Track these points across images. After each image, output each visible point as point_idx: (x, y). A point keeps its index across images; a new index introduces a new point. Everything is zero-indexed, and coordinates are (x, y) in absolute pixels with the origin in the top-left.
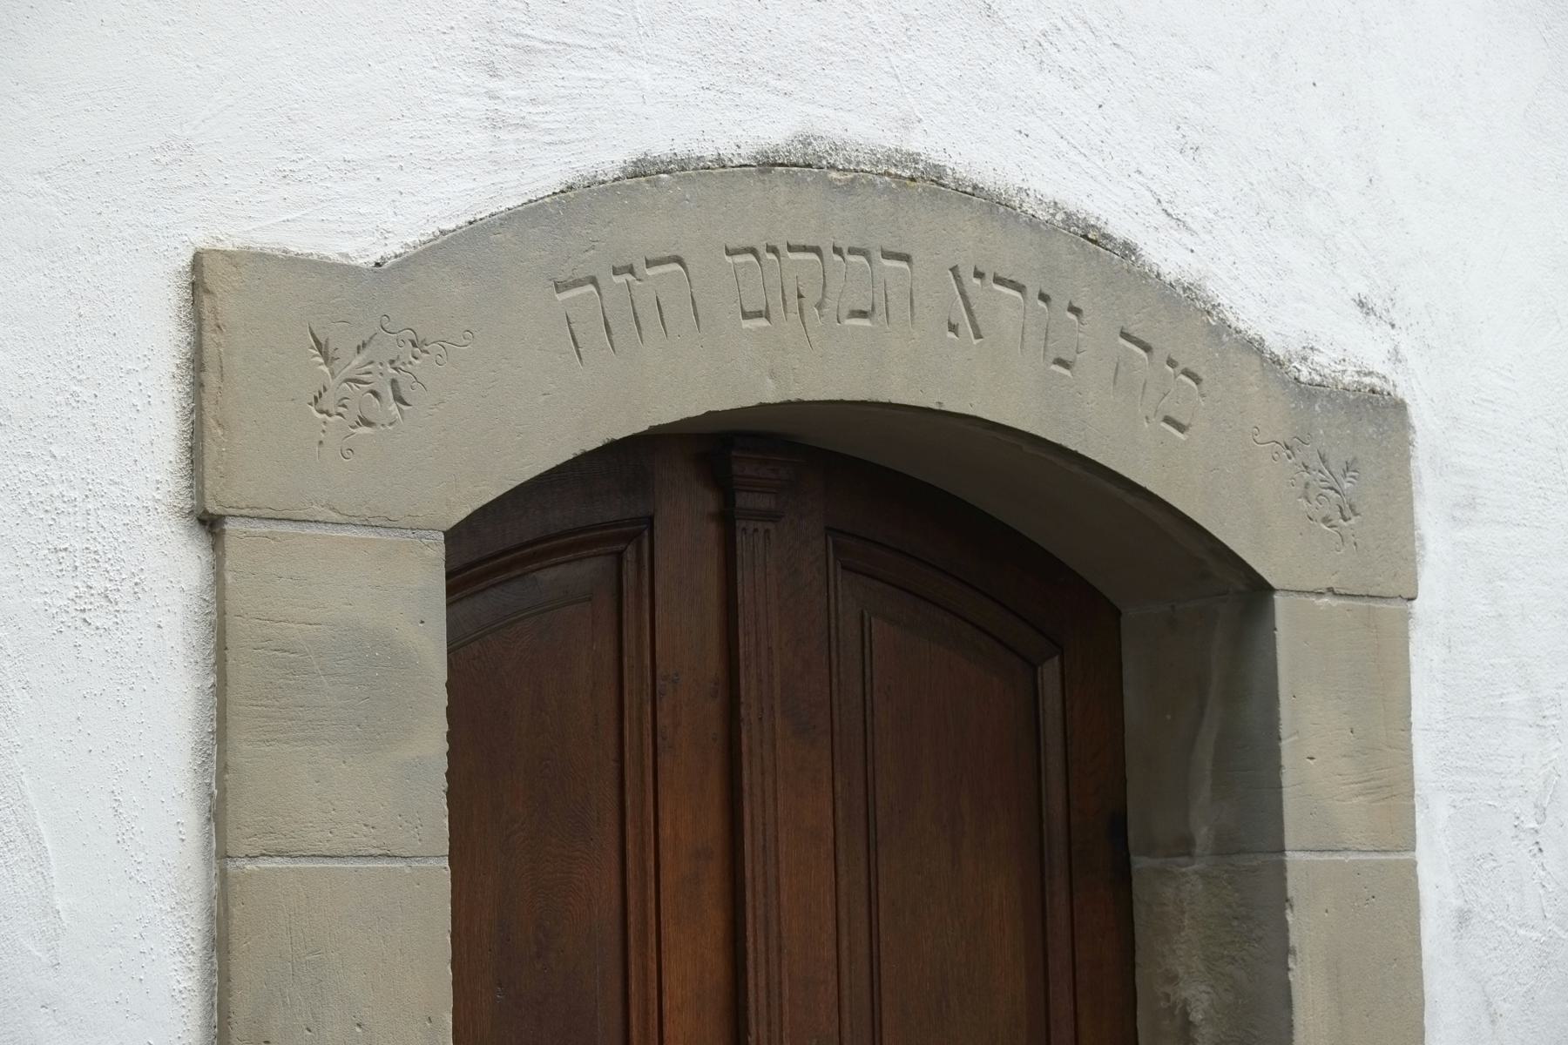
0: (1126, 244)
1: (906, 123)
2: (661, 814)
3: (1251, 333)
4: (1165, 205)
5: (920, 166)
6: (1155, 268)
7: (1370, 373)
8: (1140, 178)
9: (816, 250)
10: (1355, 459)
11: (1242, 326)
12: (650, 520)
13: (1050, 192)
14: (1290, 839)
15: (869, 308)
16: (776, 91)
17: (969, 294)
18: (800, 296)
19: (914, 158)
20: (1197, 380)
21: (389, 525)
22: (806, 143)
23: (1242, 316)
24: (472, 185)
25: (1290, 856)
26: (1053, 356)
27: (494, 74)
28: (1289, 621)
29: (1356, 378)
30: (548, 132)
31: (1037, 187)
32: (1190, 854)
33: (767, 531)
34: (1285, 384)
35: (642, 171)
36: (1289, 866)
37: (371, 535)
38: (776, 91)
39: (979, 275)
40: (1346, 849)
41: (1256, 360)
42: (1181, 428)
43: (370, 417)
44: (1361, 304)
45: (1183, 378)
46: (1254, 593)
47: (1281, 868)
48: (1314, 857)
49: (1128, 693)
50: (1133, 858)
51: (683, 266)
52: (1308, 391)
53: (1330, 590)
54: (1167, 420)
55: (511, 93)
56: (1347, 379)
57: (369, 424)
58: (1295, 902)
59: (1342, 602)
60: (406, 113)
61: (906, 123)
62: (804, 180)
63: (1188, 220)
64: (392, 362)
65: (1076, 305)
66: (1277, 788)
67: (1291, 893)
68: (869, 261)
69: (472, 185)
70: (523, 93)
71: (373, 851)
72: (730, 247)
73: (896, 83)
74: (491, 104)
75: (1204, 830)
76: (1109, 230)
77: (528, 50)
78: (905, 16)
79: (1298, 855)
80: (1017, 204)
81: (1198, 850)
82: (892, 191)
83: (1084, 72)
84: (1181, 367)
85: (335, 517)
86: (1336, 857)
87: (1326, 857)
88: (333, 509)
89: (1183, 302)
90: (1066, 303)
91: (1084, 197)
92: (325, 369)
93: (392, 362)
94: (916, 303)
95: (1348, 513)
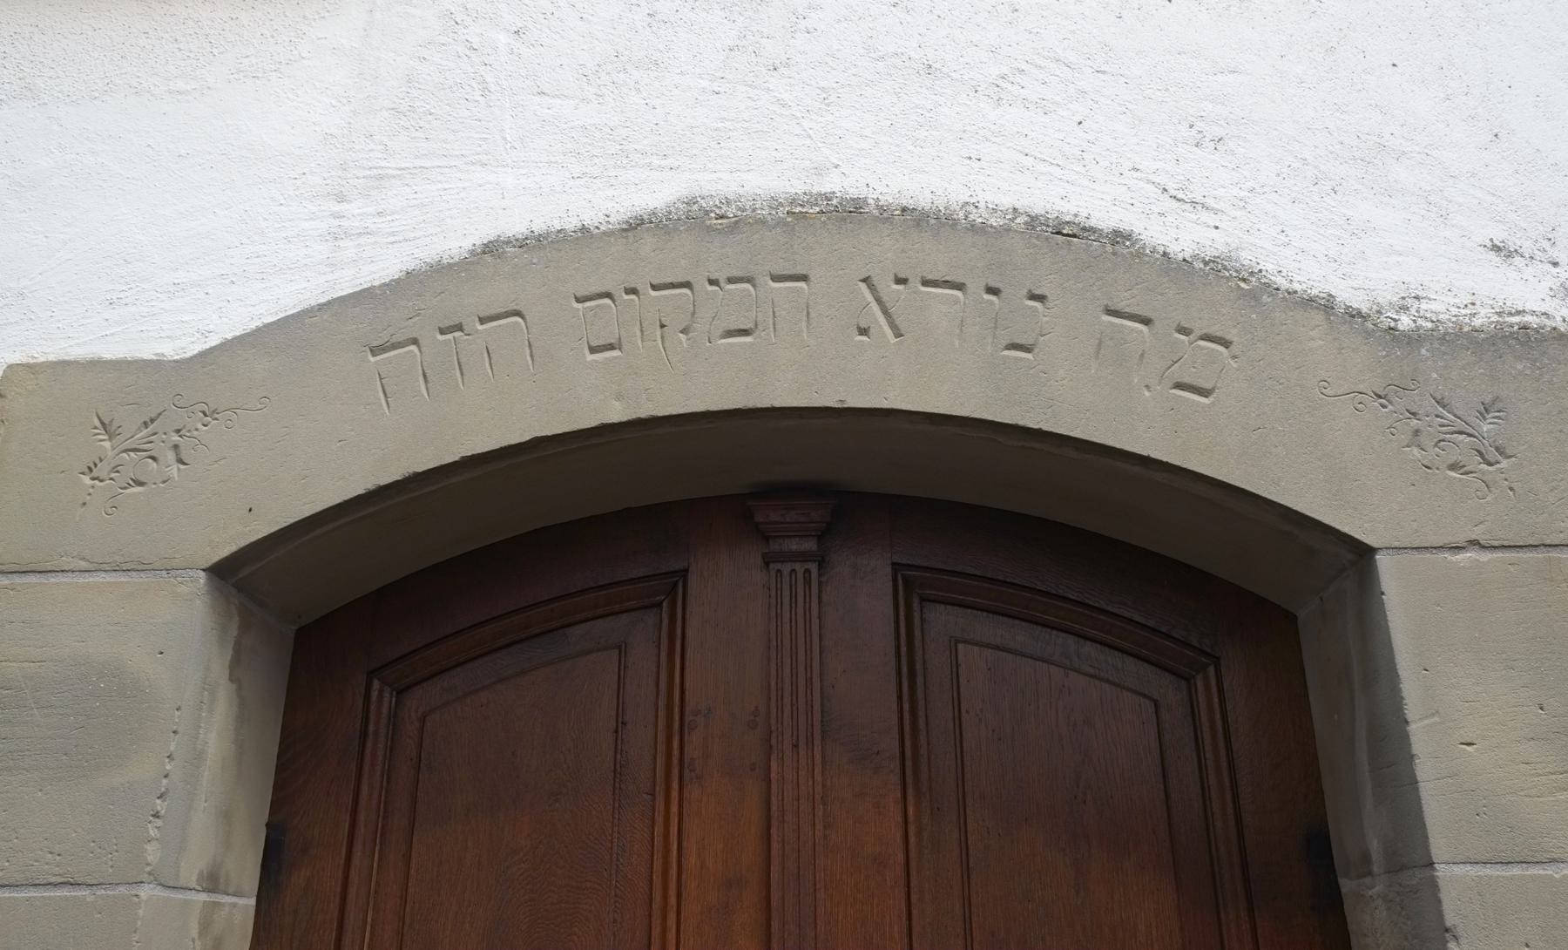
0: (1116, 233)
1: (819, 171)
2: (685, 844)
3: (1314, 292)
4: (1173, 193)
5: (835, 202)
6: (1161, 249)
7: (1518, 313)
8: (1138, 174)
9: (687, 285)
10: (1496, 399)
11: (1297, 287)
12: (686, 571)
13: (1006, 202)
14: (1439, 846)
15: (751, 325)
16: (662, 169)
17: (885, 299)
18: (662, 326)
19: (827, 198)
20: (1226, 344)
21: (143, 568)
22: (691, 201)
23: (1296, 278)
24: (305, 285)
25: (1442, 871)
26: (1005, 343)
27: (341, 199)
28: (1394, 579)
29: (1495, 318)
30: (393, 234)
31: (989, 199)
32: (1370, 874)
33: (807, 571)
34: (1368, 334)
35: (492, 249)
36: (1441, 883)
37: (123, 578)
38: (662, 169)
39: (901, 281)
40: (1553, 861)
41: (1318, 317)
42: (1028, 349)
43: (142, 479)
44: (1496, 248)
45: (1202, 343)
46: (1358, 557)
47: (1433, 885)
48: (1488, 871)
49: (1311, 698)
50: (1342, 881)
51: (522, 317)
52: (1413, 339)
53: (1474, 543)
54: (1179, 386)
55: (357, 211)
56: (1477, 322)
57: (141, 484)
58: (1460, 932)
59: (1498, 555)
60: (245, 240)
61: (819, 171)
62: (675, 230)
63: (1210, 202)
64: (178, 431)
65: (1038, 292)
66: (1414, 782)
67: (1450, 919)
68: (754, 286)
69: (305, 285)
70: (371, 210)
71: (53, 879)
72: (579, 295)
73: (808, 142)
74: (336, 222)
75: (1375, 842)
76: (1093, 223)
77: (381, 177)
78: (823, 89)
79: (1459, 870)
80: (961, 215)
81: (1375, 869)
82: (787, 224)
83: (1057, 98)
84: (1198, 333)
85: (83, 565)
86: (1549, 871)
87: (1516, 871)
88: (83, 559)
89: (1211, 274)
90: (1025, 292)
91: (1058, 201)
92: (107, 444)
93: (178, 431)
94: (813, 315)
95: (1492, 455)
